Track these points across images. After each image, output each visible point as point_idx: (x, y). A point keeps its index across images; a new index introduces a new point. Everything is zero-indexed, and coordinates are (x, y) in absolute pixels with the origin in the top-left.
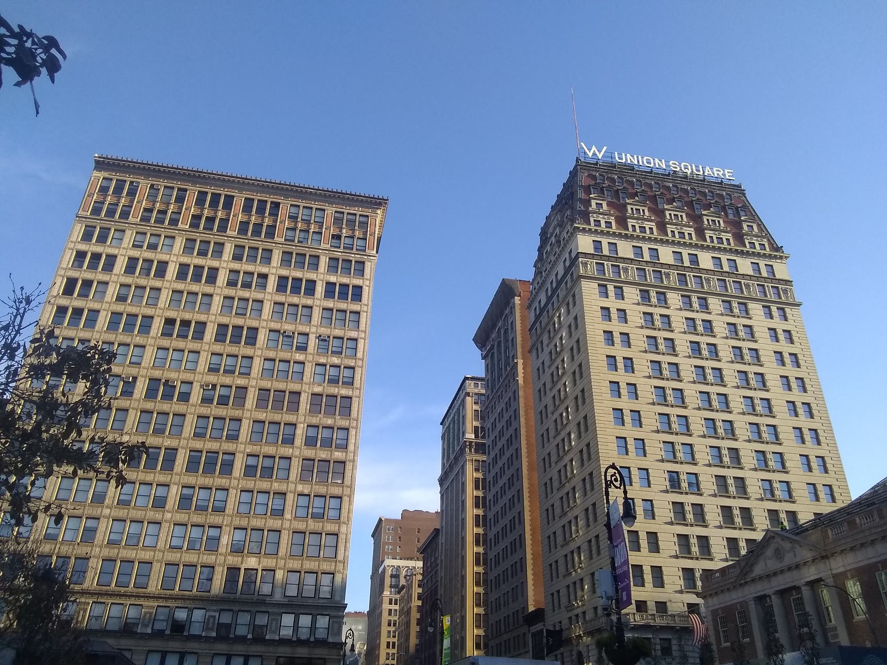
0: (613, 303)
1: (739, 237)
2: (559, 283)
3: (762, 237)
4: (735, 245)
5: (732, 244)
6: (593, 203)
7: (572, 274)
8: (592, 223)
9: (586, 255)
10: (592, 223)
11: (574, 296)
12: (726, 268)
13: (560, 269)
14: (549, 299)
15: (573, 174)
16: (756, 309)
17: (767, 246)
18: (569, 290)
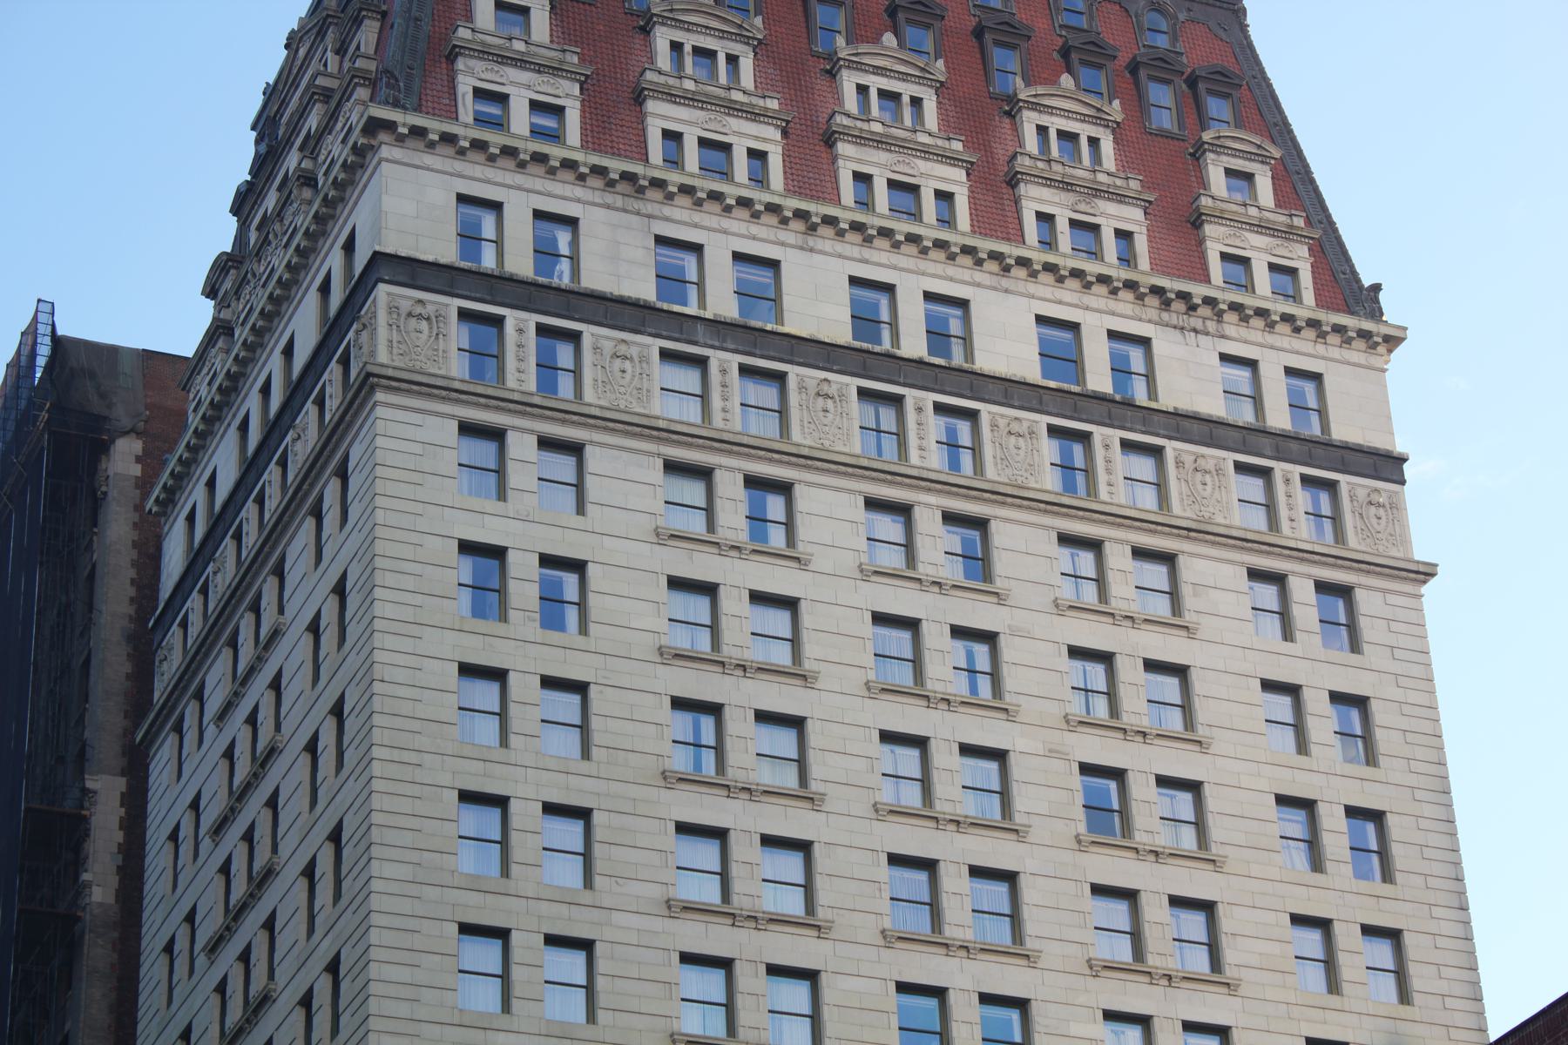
0: (528, 522)
1: (1182, 223)
2: (298, 391)
3: (1288, 234)
4: (1156, 267)
5: (1144, 263)
7: (345, 362)
8: (467, 107)
9: (413, 271)
10: (467, 107)
11: (343, 474)
12: (1099, 379)
14: (251, 468)
16: (1214, 579)
17: (1306, 277)
18: (336, 433)
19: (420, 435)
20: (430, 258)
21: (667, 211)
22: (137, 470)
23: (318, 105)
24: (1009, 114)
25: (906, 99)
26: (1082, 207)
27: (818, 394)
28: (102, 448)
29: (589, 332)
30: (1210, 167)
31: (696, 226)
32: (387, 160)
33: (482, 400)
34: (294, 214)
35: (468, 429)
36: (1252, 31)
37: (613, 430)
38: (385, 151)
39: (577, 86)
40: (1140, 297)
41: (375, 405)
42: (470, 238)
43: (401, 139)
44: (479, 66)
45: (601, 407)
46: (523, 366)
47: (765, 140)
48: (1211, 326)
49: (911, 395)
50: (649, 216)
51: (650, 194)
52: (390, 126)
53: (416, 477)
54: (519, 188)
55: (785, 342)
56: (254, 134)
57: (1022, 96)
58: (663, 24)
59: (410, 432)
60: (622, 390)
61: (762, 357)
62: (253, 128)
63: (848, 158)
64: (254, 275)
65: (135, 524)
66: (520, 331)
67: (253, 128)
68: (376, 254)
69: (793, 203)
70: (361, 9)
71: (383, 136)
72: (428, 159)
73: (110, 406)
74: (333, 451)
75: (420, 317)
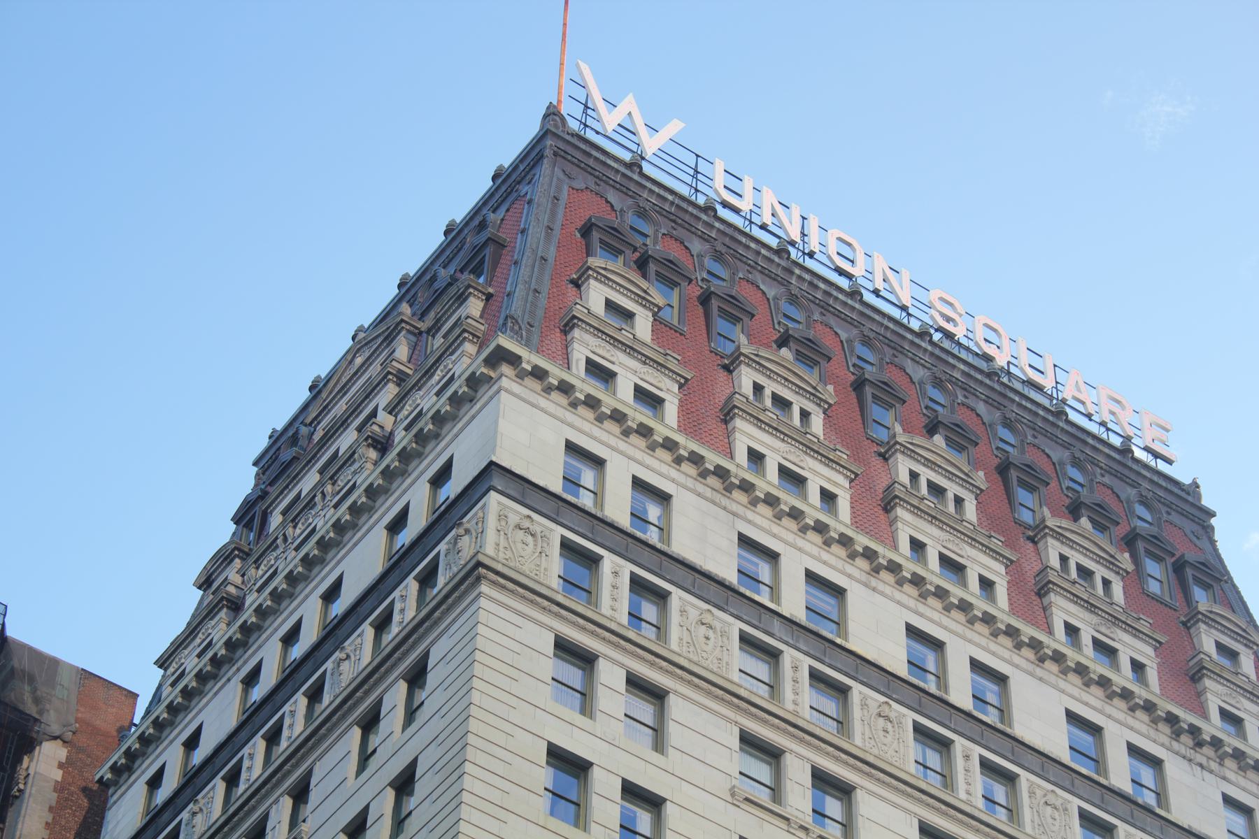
0: (614, 746)
6: (596, 296)
9: (525, 489)
13: (362, 563)
15: (509, 185)
19: (518, 634)
20: (541, 483)
21: (750, 515)
22: (58, 775)
23: (391, 386)
24: (1032, 540)
25: (950, 495)
26: (1103, 629)
27: (880, 715)
28: (28, 745)
29: (678, 597)
30: (1203, 636)
31: (775, 536)
32: (506, 391)
33: (581, 621)
34: (355, 473)
35: (564, 648)
36: (1220, 546)
37: (697, 686)
38: (505, 382)
39: (677, 386)
40: (1155, 721)
41: (479, 595)
42: (571, 482)
43: (522, 375)
44: (593, 341)
45: (690, 661)
46: (617, 605)
47: (836, 484)
48: (1214, 766)
49: (960, 744)
50: (734, 514)
51: (737, 494)
52: (514, 360)
53: (515, 673)
54: (621, 453)
55: (851, 659)
56: (256, 469)
57: (1049, 523)
58: (748, 365)
59: (510, 630)
60: (704, 654)
61: (830, 666)
62: (255, 464)
63: (906, 523)
64: (285, 539)
65: (47, 823)
66: (616, 573)
67: (255, 464)
68: (492, 463)
69: (862, 541)
70: (469, 286)
71: (505, 369)
72: (543, 402)
73: (41, 712)
74: (367, 693)
75: (527, 530)
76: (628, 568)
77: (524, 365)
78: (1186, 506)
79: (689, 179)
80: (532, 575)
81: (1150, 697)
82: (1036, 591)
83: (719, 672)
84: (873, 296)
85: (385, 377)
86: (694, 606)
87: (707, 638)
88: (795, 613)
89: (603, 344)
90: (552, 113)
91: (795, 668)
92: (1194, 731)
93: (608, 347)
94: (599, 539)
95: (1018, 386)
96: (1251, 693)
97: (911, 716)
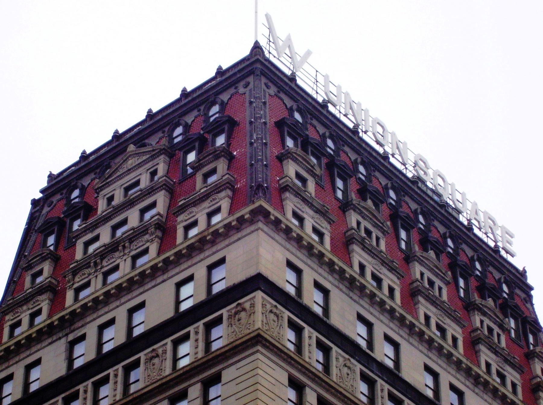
44: (296, 200)
47: (394, 282)
52: (267, 214)
59: (269, 371)
60: (346, 383)
63: (423, 305)
75: (275, 314)
76: (315, 334)
77: (315, 250)
78: (518, 280)
79: (312, 84)
80: (277, 339)
81: (394, 306)
82: (345, 243)
83: (352, 393)
84: (478, 230)
85: (162, 186)
86: (270, 303)
87: (348, 374)
88: (290, 291)
89: (300, 201)
90: (257, 47)
91: (382, 390)
92: (342, 272)
93: (302, 203)
94: (275, 297)
95: (430, 193)
96: (370, 251)
97: (287, 314)
